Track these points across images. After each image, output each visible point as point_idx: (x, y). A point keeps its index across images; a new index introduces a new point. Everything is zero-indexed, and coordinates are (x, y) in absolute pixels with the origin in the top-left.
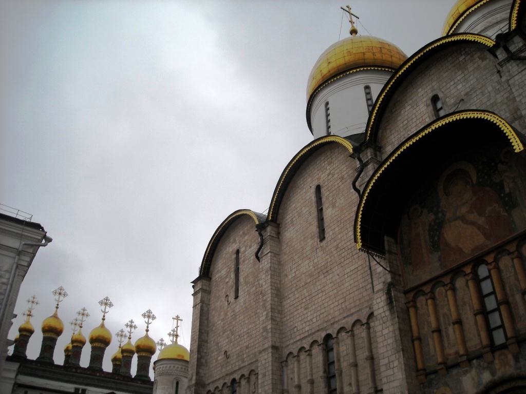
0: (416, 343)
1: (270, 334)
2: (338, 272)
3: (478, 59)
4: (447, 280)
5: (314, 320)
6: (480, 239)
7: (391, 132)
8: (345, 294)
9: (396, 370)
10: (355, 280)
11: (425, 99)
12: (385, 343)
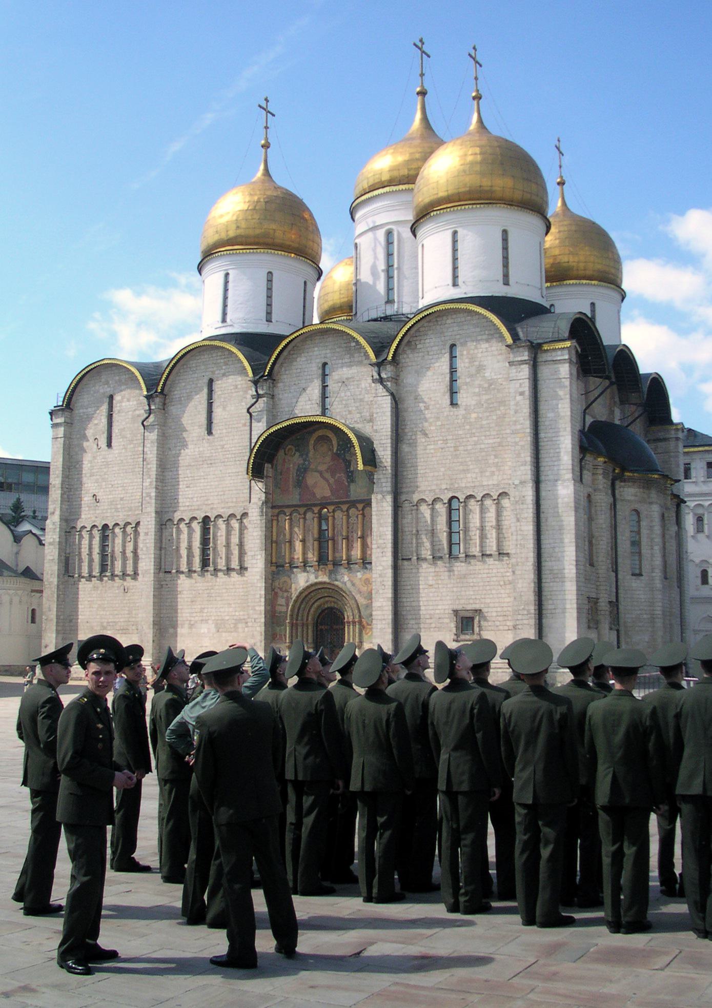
0: (274, 545)
1: (153, 501)
2: (221, 468)
3: (362, 354)
4: (302, 510)
5: (195, 500)
6: (327, 493)
7: (286, 371)
8: (224, 489)
9: (258, 561)
10: (235, 481)
11: (318, 361)
12: (254, 541)
